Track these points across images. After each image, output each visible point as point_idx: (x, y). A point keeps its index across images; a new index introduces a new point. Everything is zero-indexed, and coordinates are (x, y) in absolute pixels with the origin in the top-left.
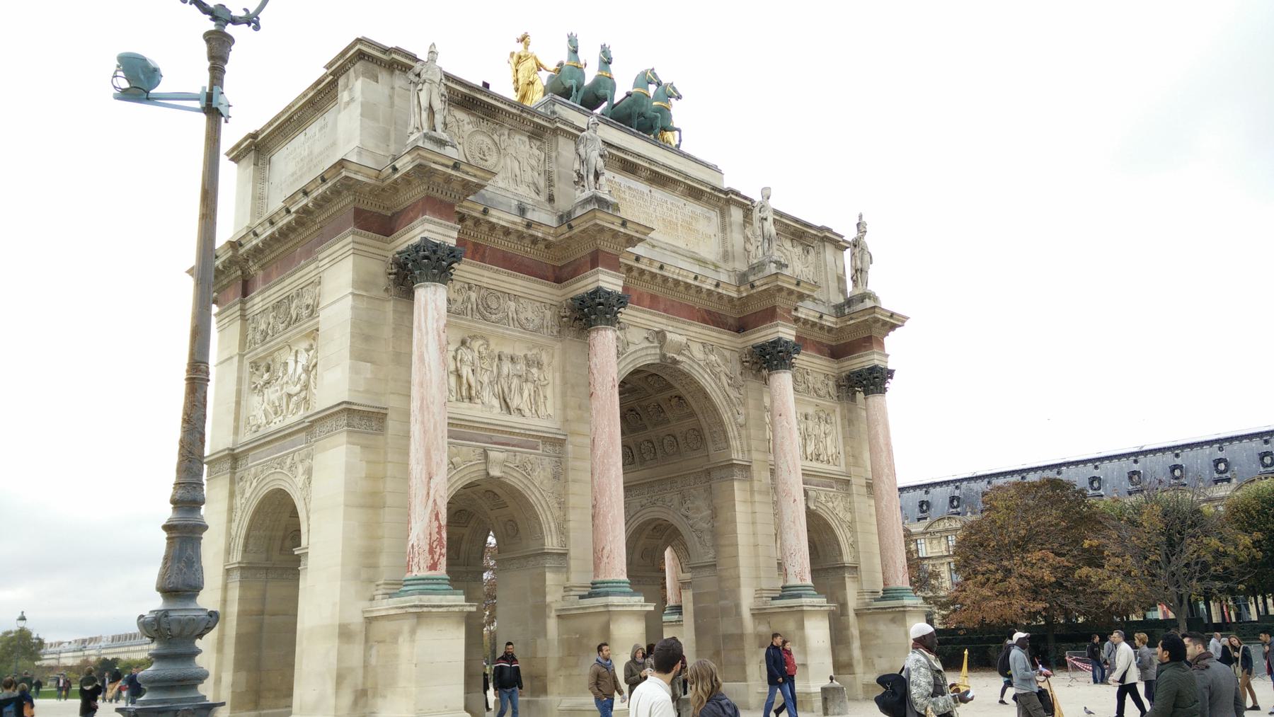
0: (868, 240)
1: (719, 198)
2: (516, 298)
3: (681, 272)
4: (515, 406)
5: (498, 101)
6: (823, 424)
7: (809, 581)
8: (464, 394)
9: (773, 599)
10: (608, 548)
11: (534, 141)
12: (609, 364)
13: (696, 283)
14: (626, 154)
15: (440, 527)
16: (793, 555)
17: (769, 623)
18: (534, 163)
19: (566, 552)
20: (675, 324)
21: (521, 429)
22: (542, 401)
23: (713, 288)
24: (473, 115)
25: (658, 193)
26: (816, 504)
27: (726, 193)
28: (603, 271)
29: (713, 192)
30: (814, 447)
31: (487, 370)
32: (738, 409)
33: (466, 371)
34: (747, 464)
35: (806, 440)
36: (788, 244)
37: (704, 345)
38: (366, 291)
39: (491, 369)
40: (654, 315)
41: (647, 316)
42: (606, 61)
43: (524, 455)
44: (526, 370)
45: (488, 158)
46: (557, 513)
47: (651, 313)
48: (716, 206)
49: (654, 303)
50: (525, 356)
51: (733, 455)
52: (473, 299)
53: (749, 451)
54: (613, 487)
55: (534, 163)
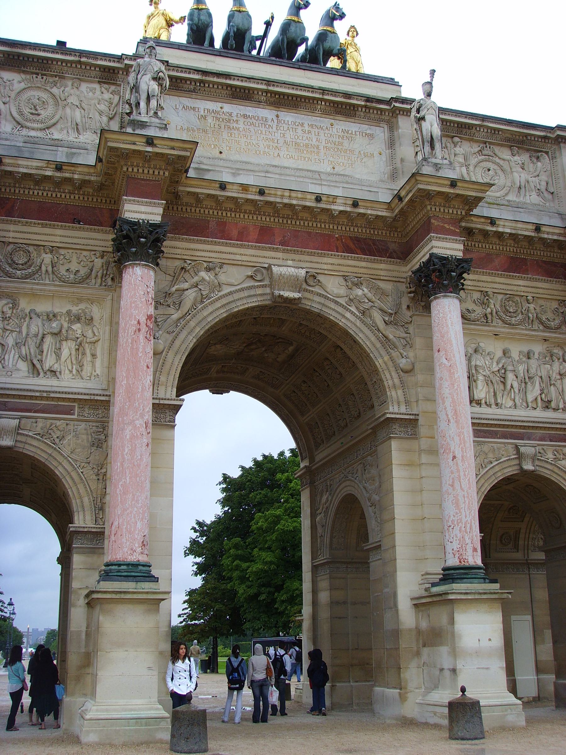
0: (433, 83)
1: (381, 110)
2: (52, 250)
3: (293, 194)
4: (47, 366)
5: (47, 51)
6: (556, 365)
7: (475, 559)
9: (434, 585)
10: (116, 524)
11: (105, 86)
12: (133, 305)
13: (322, 205)
14: (230, 79)
16: (450, 528)
17: (429, 616)
19: (103, 530)
20: (297, 257)
21: (43, 391)
22: (89, 357)
23: (348, 209)
24: (24, 72)
26: (537, 463)
27: (388, 102)
28: (130, 200)
29: (368, 104)
30: (539, 392)
31: (12, 331)
32: (402, 351)
34: (412, 417)
35: (526, 383)
36: (505, 153)
37: (345, 278)
39: (18, 330)
40: (263, 249)
43: (51, 421)
44: (69, 327)
45: (42, 112)
46: (93, 486)
47: (256, 248)
48: (380, 120)
50: (69, 312)
51: (391, 408)
53: (417, 401)
54: (126, 450)
55: (102, 107)
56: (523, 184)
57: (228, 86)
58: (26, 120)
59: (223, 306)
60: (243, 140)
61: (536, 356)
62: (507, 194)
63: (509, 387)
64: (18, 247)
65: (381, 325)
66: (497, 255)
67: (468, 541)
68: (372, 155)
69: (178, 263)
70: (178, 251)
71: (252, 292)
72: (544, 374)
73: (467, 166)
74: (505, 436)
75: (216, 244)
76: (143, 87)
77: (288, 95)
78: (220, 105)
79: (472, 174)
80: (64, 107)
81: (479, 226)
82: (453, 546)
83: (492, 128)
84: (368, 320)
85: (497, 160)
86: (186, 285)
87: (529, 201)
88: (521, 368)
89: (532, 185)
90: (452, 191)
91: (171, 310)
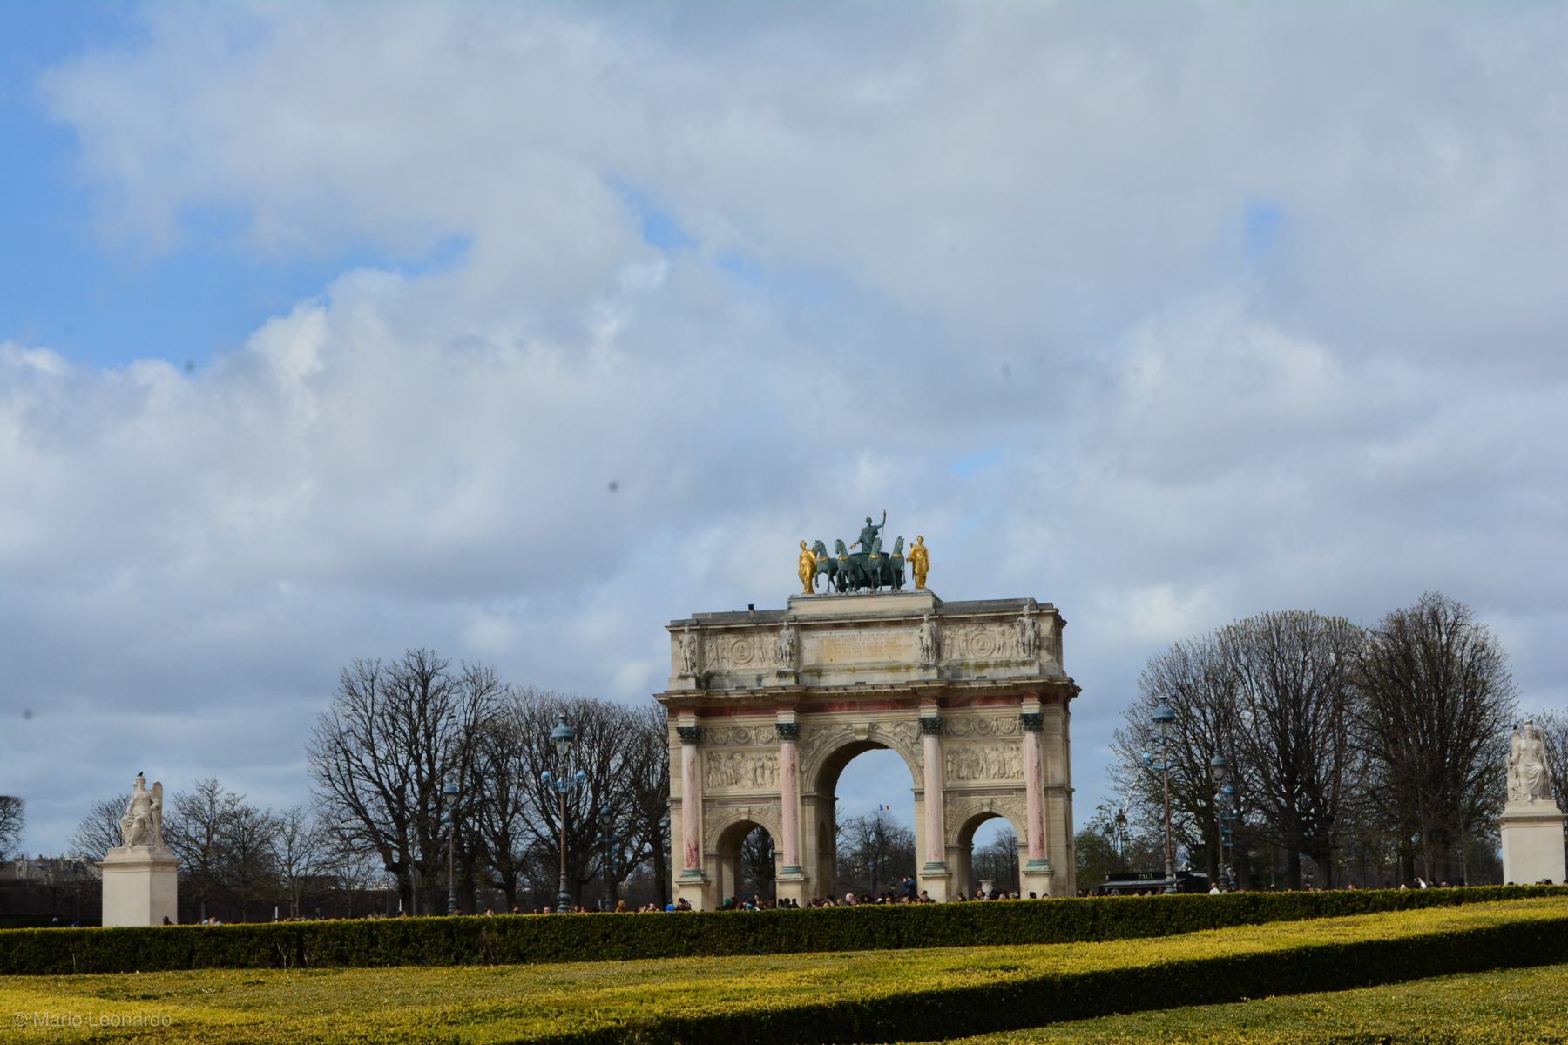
15: (691, 850)
18: (772, 646)
20: (868, 715)
25: (866, 633)
27: (917, 616)
33: (730, 771)
42: (840, 547)
52: (730, 735)
58: (738, 659)
62: (991, 654)
63: (980, 768)
65: (909, 745)
69: (812, 727)
72: (1001, 759)
73: (967, 641)
76: (783, 648)
80: (754, 649)
82: (928, 853)
84: (904, 743)
85: (987, 632)
86: (815, 738)
87: (1004, 656)
89: (1008, 645)
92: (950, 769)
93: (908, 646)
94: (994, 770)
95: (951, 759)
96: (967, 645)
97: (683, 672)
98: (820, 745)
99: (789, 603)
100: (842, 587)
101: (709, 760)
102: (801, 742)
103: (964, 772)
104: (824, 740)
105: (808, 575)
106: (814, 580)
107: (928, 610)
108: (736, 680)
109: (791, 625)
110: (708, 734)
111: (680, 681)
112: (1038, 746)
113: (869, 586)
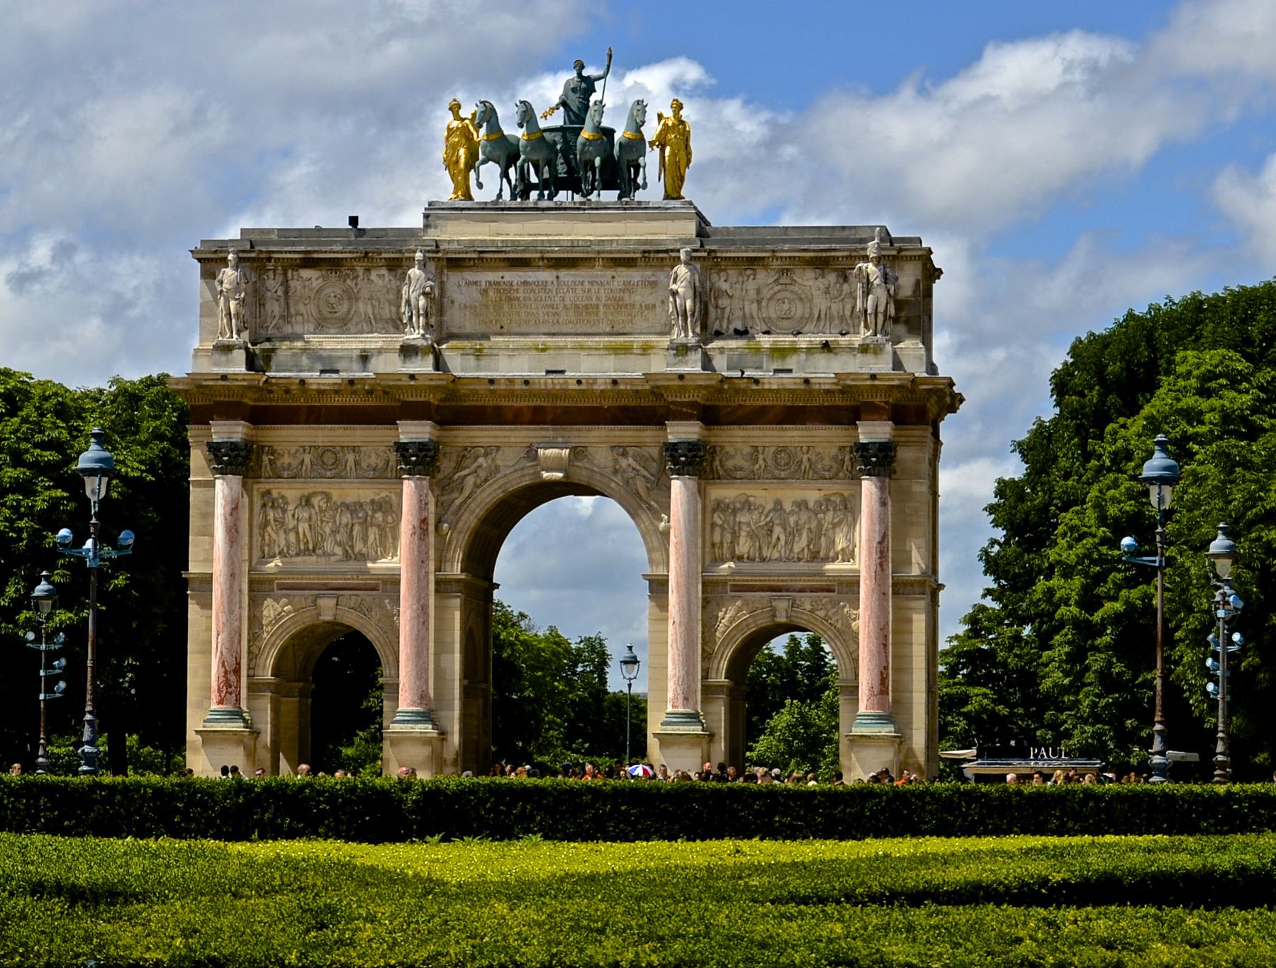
1: (662, 259)
2: (355, 449)
8: (302, 547)
15: (226, 672)
20: (566, 434)
22: (391, 541)
25: (567, 275)
27: (667, 251)
30: (806, 543)
31: (328, 522)
33: (303, 527)
38: (203, 476)
40: (535, 430)
41: (525, 433)
49: (538, 416)
50: (373, 501)
56: (823, 312)
57: (505, 259)
59: (500, 487)
60: (522, 311)
61: (811, 505)
63: (774, 540)
64: (326, 449)
66: (773, 407)
67: (680, 692)
68: (654, 306)
70: (460, 440)
71: (526, 472)
72: (814, 525)
73: (759, 302)
74: (762, 589)
75: (492, 430)
76: (413, 301)
77: (565, 259)
78: (501, 274)
79: (763, 310)
80: (357, 300)
81: (743, 386)
83: (786, 258)
85: (796, 288)
88: (792, 520)
90: (681, 383)
91: (455, 495)
92: (717, 538)
93: (647, 307)
94: (801, 543)
95: (720, 522)
96: (759, 309)
97: (225, 340)
98: (477, 486)
99: (426, 216)
100: (524, 189)
101: (264, 505)
102: (439, 476)
103: (743, 547)
104: (483, 474)
105: (462, 165)
106: (472, 174)
107: (687, 242)
108: (320, 358)
109: (430, 258)
110: (265, 459)
111: (217, 356)
112: (883, 504)
113: (577, 190)
